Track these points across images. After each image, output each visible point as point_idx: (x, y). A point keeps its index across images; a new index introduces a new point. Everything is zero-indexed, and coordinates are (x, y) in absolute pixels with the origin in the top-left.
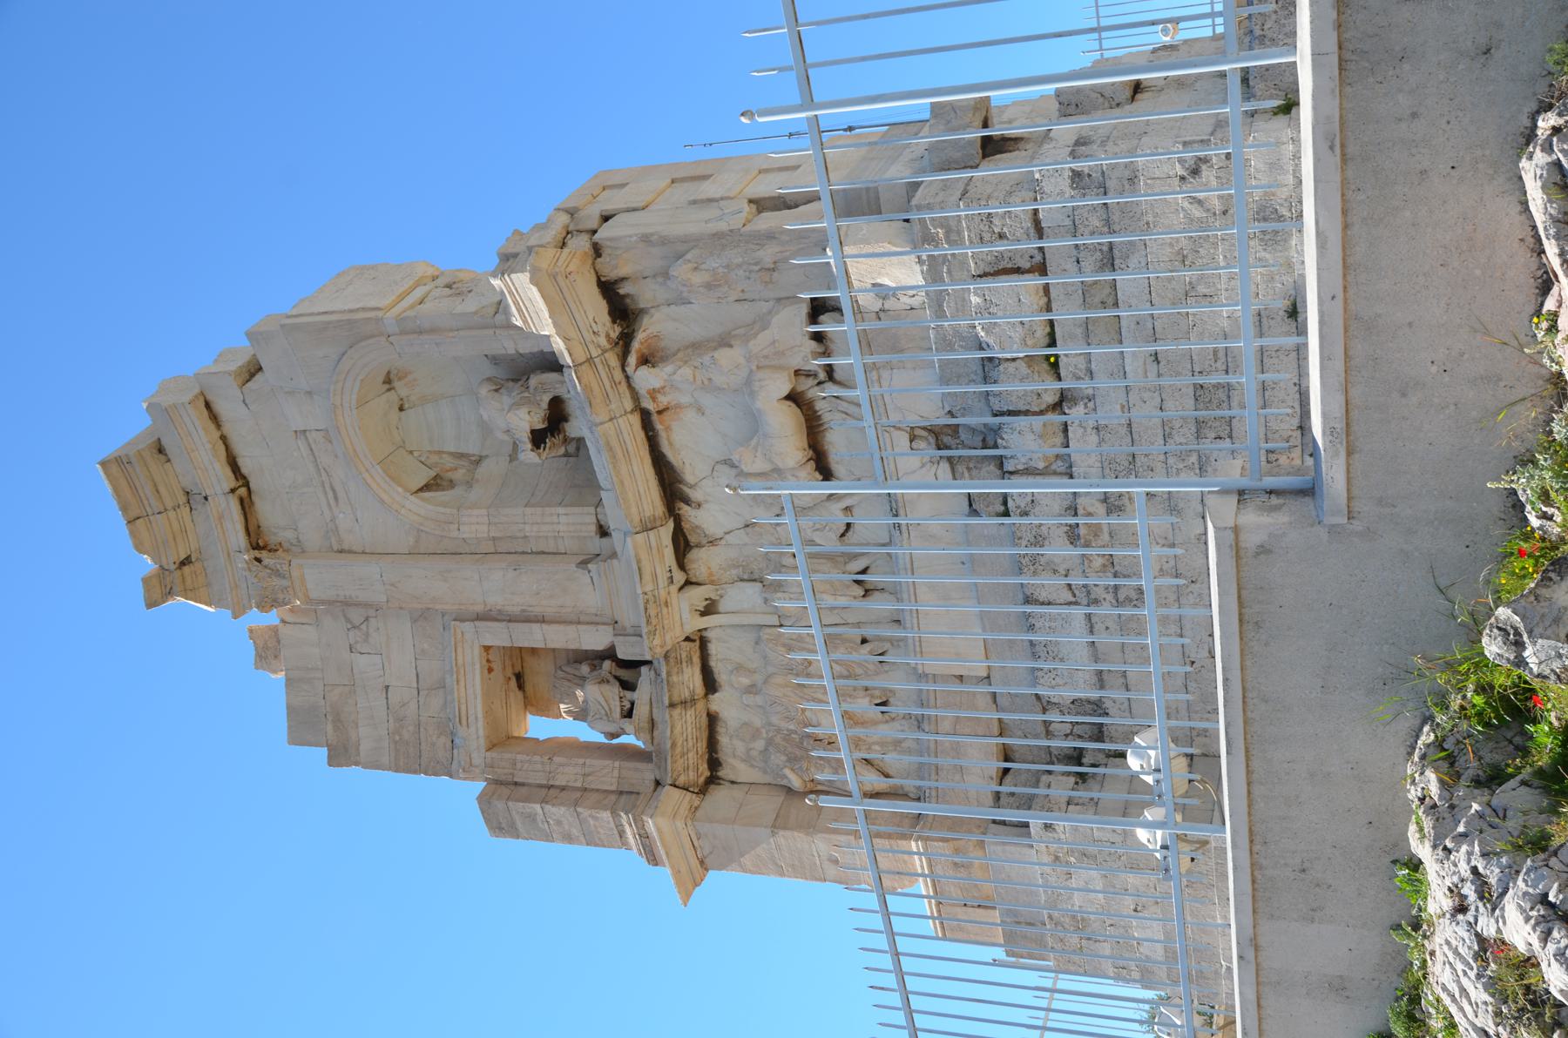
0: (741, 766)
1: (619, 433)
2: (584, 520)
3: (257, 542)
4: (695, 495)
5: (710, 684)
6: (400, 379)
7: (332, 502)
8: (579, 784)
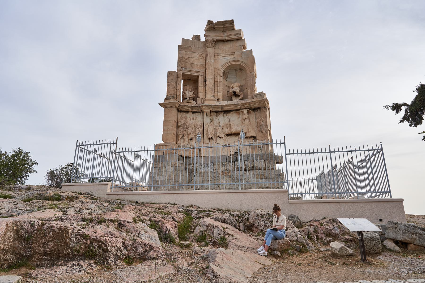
0: (180, 116)
1: (238, 106)
2: (220, 97)
3: (218, 41)
4: (225, 115)
5: (194, 113)
7: (223, 56)
8: (178, 89)
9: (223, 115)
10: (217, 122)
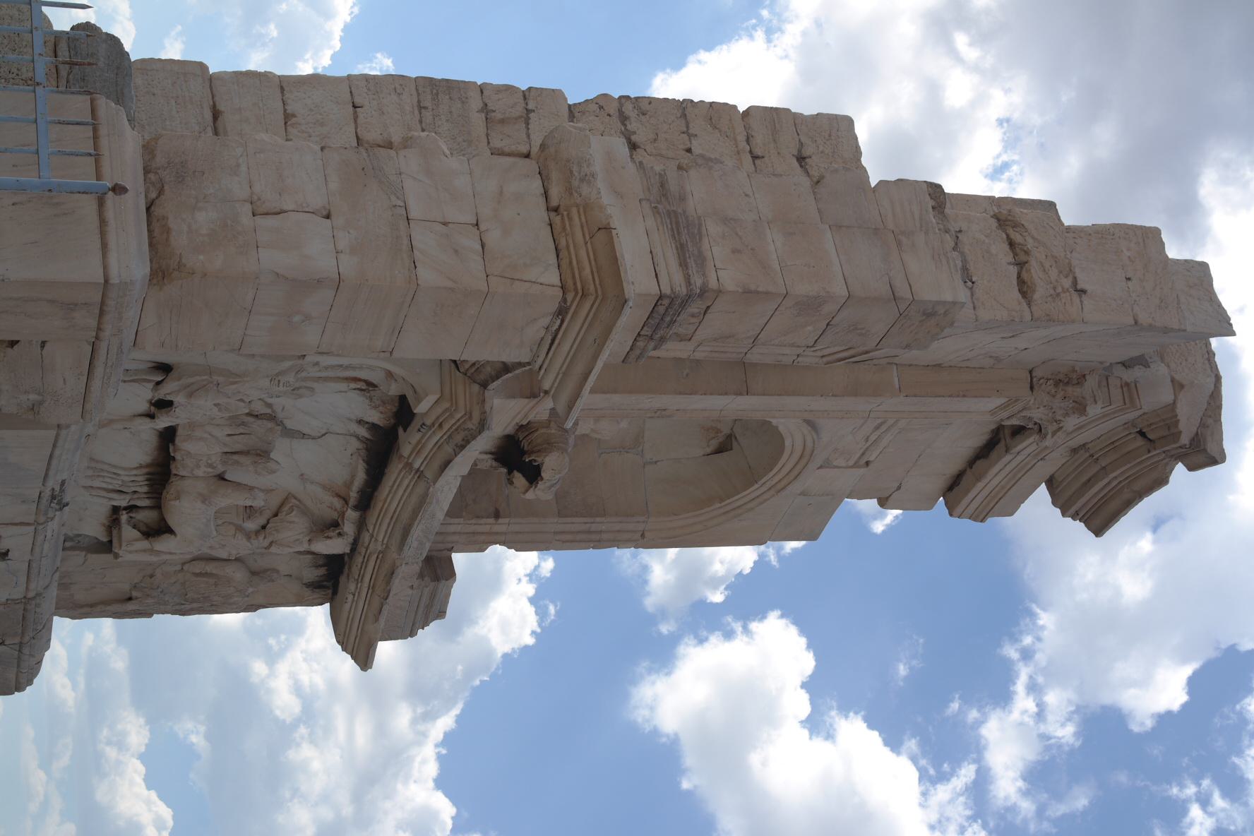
6: (718, 431)
9: (360, 422)
10: (315, 385)
